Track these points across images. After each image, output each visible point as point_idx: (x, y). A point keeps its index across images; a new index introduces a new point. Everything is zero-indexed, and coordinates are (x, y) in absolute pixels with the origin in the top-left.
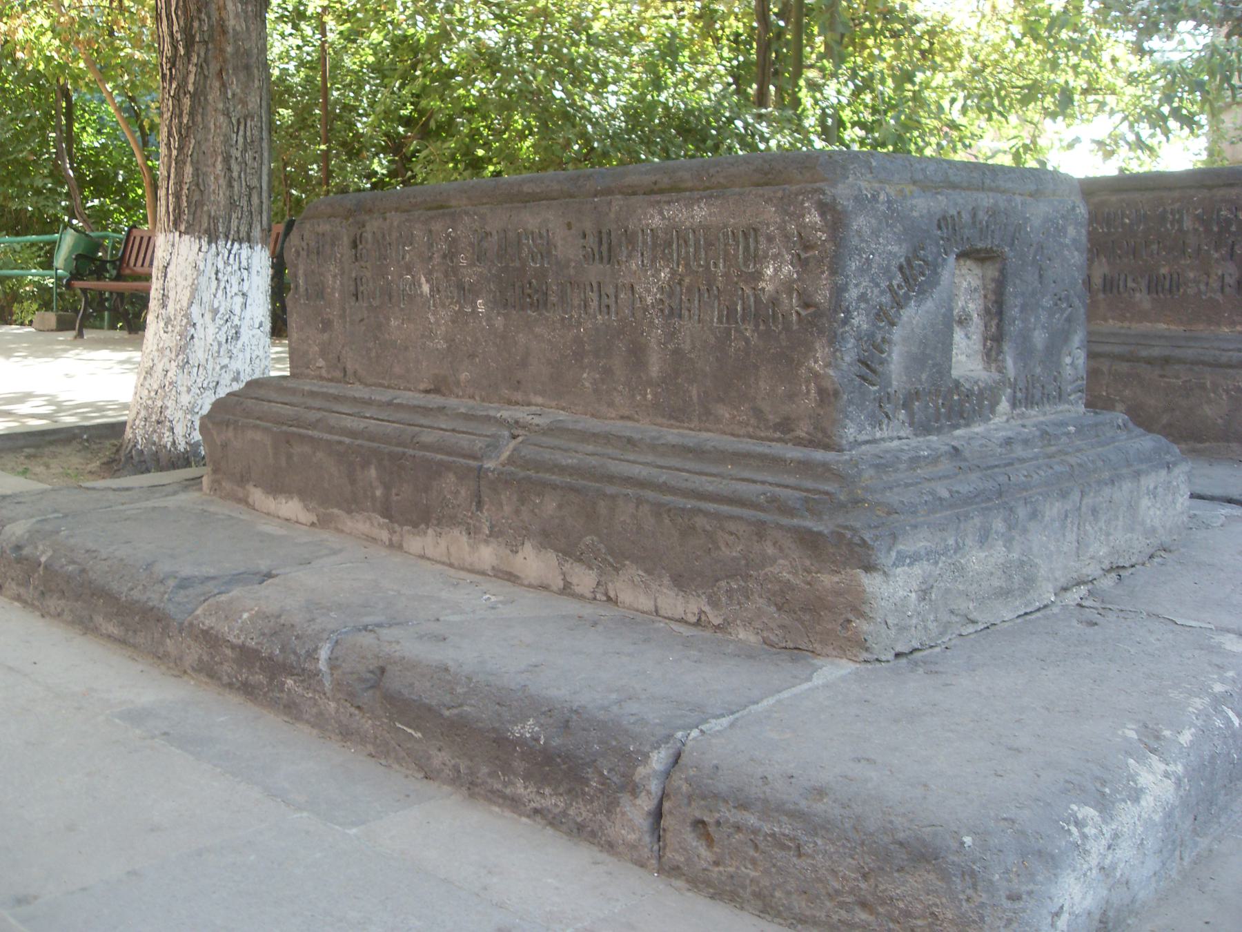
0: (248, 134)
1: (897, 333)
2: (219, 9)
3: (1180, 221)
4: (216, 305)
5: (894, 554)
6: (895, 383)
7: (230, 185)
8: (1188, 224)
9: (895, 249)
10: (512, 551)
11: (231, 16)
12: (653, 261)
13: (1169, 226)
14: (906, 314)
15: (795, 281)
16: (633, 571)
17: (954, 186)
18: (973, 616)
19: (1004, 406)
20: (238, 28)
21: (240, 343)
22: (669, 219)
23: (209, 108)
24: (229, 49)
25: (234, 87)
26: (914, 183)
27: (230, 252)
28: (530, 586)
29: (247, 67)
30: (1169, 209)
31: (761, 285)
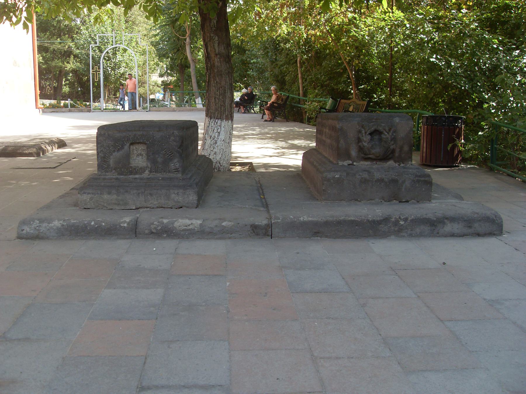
0: (221, 92)
1: (112, 157)
2: (213, 61)
4: (211, 135)
5: (83, 192)
6: (112, 166)
7: (216, 105)
9: (111, 143)
11: (216, 62)
14: (114, 154)
17: (129, 131)
18: (107, 206)
19: (147, 172)
20: (218, 65)
21: (217, 145)
23: (211, 85)
24: (216, 71)
25: (217, 80)
26: (117, 131)
27: (215, 122)
29: (221, 75)
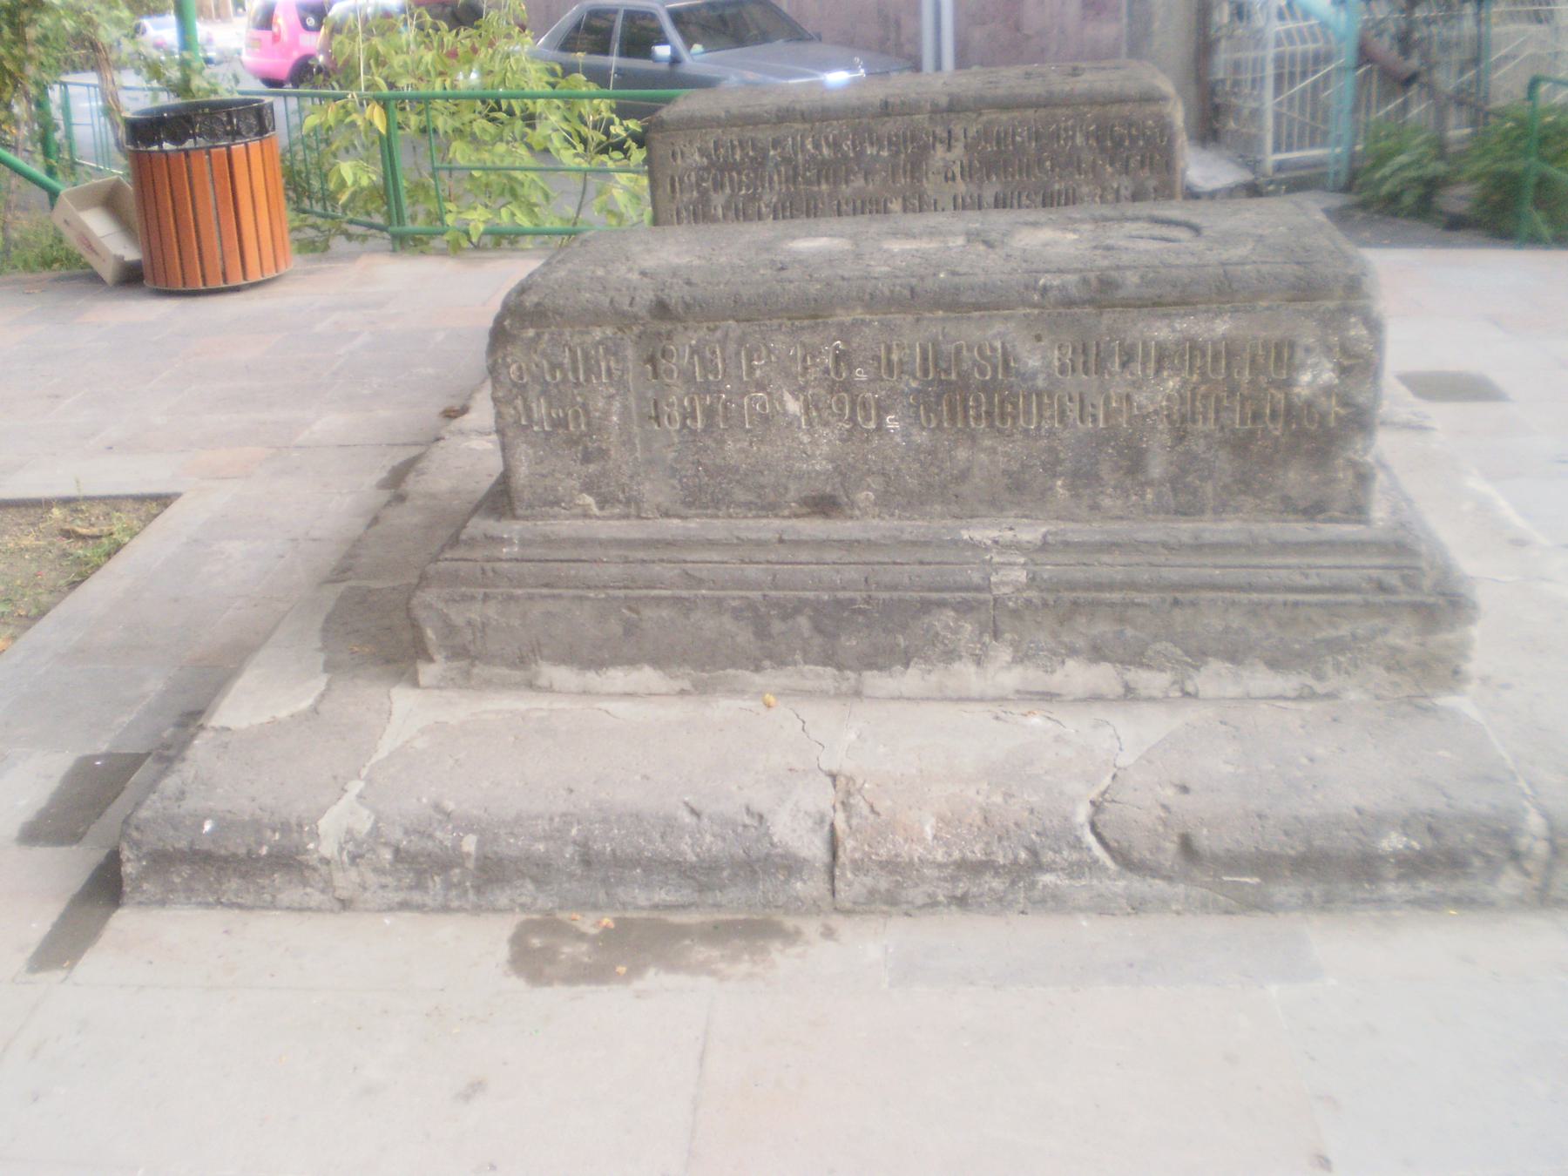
3: (1073, 138)
8: (1079, 140)
10: (1047, 672)
12: (1158, 371)
13: (1062, 142)
15: (1336, 386)
16: (1215, 665)
22: (1181, 331)
28: (1076, 700)
30: (1063, 125)
31: (1297, 390)
